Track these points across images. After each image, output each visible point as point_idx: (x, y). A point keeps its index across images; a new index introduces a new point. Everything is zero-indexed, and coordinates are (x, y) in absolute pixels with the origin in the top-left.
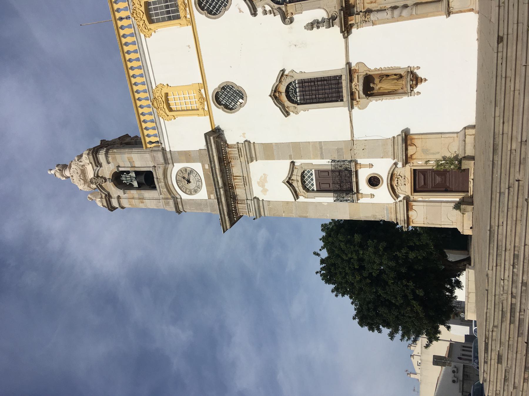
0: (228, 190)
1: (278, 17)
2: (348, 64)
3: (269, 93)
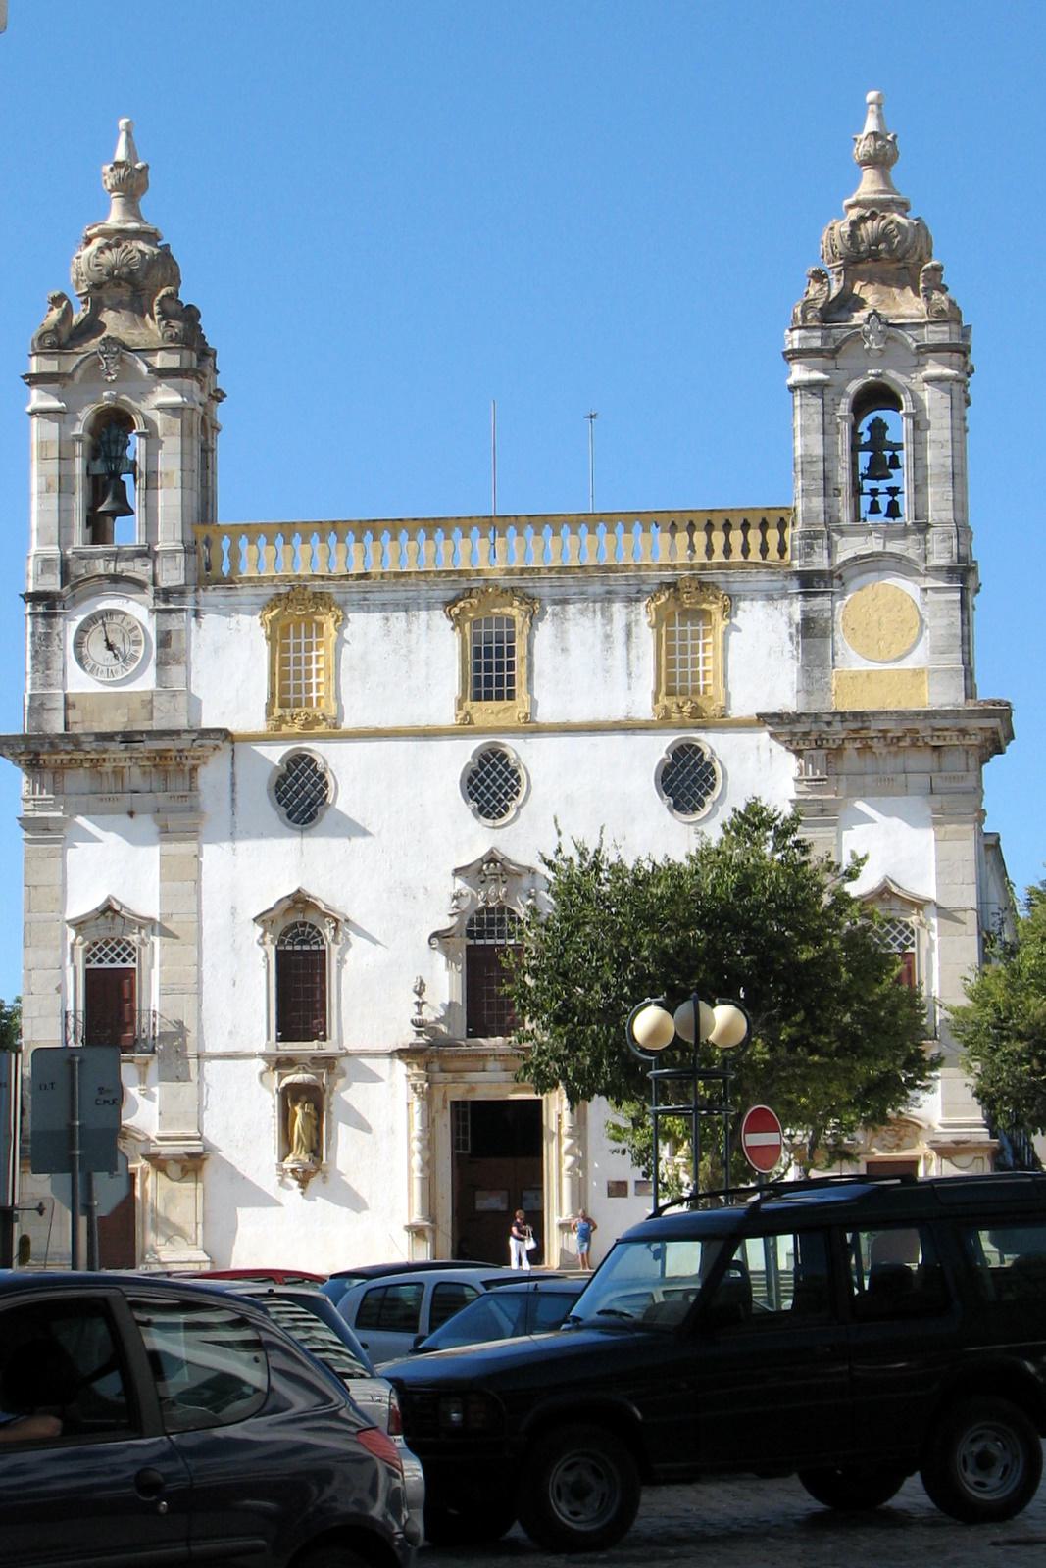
0: (92, 757)
1: (446, 923)
2: (348, 1054)
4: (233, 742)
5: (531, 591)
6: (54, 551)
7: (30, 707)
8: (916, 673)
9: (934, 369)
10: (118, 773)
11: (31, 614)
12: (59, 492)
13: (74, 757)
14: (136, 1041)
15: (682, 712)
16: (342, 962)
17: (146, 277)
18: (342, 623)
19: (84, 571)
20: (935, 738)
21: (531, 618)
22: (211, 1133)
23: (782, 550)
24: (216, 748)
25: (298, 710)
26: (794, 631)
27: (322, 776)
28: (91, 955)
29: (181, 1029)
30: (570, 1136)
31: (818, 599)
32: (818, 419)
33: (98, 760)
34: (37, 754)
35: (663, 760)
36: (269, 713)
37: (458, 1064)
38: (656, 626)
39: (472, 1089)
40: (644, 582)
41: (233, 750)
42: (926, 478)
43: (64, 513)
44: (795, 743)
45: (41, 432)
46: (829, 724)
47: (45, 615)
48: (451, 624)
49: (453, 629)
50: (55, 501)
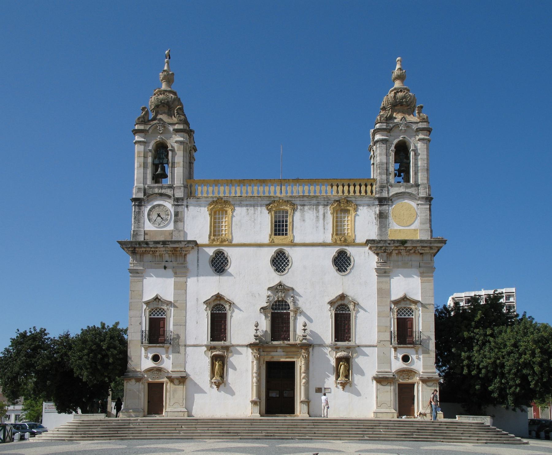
1: (265, 305)
2: (233, 346)
3: (220, 293)
4: (198, 247)
5: (293, 202)
6: (142, 185)
7: (133, 234)
8: (415, 230)
9: (421, 136)
10: (161, 256)
11: (134, 205)
12: (144, 167)
13: (147, 250)
14: (165, 340)
15: (341, 241)
16: (231, 316)
17: (173, 104)
18: (233, 210)
19: (151, 192)
21: (293, 210)
22: (189, 370)
23: (372, 192)
24: (193, 248)
25: (219, 237)
26: (376, 216)
27: (226, 258)
28: (151, 313)
29: (178, 337)
30: (304, 373)
31: (384, 206)
32: (385, 151)
33: (154, 251)
34: (135, 248)
35: (335, 255)
36: (210, 238)
37: (269, 350)
38: (333, 214)
39: (273, 357)
40: (329, 200)
41: (198, 249)
42: (418, 171)
43: (145, 174)
45: (138, 149)
46: (389, 244)
47: (138, 206)
48: (268, 212)
49: (269, 213)
50: (142, 170)
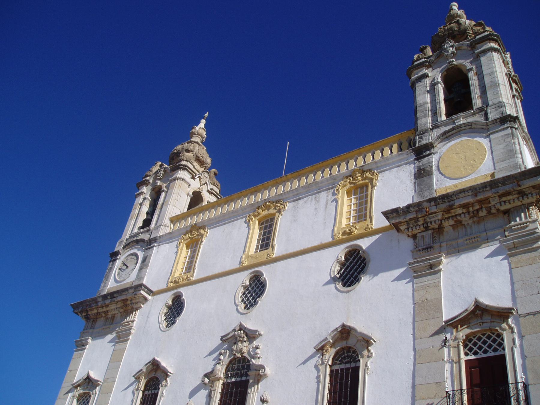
20: (503, 203)
44: (410, 230)
